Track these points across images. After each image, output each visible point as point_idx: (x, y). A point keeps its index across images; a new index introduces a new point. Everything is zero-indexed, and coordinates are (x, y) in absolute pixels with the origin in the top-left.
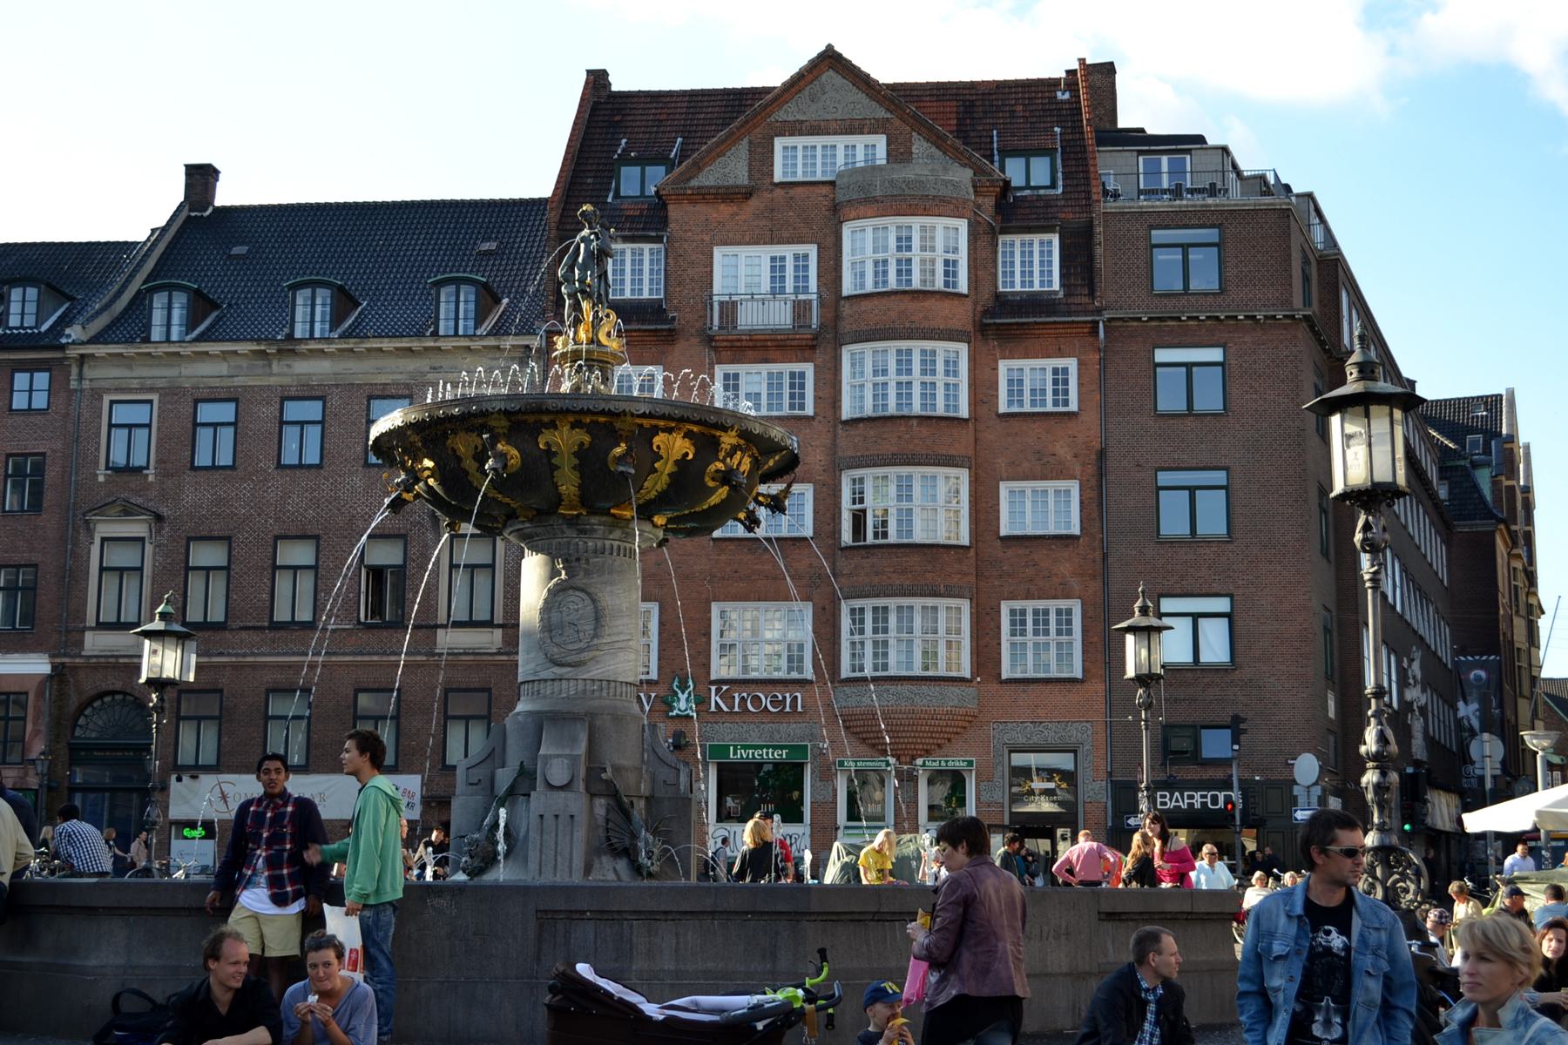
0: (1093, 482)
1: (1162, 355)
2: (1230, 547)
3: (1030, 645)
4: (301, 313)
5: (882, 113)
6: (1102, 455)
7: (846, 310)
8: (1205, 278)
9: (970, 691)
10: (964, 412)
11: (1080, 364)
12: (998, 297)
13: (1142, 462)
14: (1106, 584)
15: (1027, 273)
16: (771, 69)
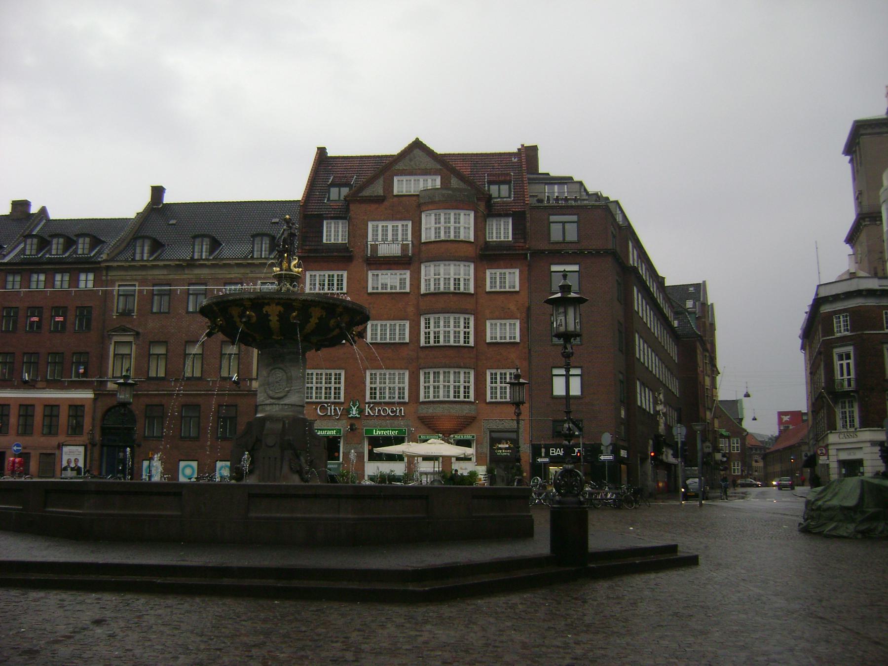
1: (554, 268)
3: (499, 388)
4: (138, 250)
5: (439, 167)
6: (529, 309)
7: (423, 248)
8: (572, 234)
9: (473, 407)
10: (472, 291)
12: (486, 243)
14: (530, 362)
15: (498, 233)
16: (394, 148)
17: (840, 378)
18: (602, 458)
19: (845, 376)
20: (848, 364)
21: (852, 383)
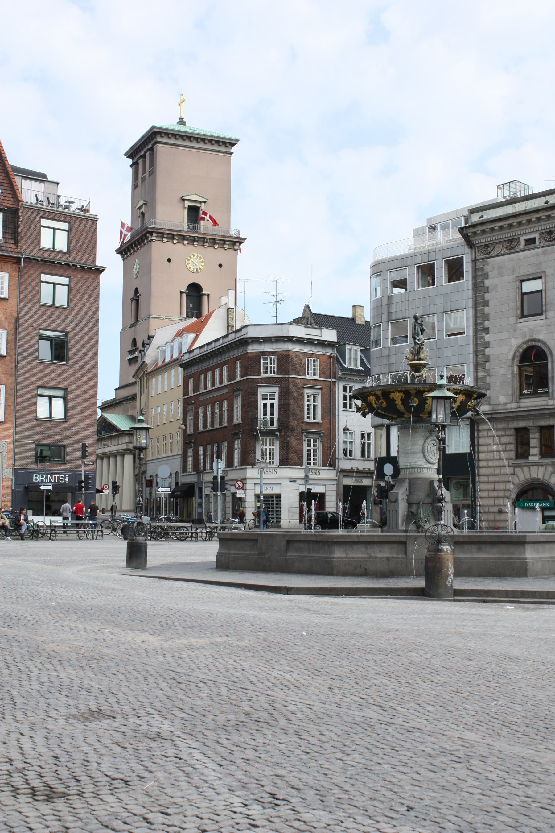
0: (13, 332)
1: (44, 277)
2: (67, 367)
6: (17, 319)
8: (62, 244)
11: (10, 276)
13: (34, 325)
14: (16, 379)
17: (262, 416)
18: (160, 490)
19: (268, 416)
20: (272, 405)
21: (275, 422)
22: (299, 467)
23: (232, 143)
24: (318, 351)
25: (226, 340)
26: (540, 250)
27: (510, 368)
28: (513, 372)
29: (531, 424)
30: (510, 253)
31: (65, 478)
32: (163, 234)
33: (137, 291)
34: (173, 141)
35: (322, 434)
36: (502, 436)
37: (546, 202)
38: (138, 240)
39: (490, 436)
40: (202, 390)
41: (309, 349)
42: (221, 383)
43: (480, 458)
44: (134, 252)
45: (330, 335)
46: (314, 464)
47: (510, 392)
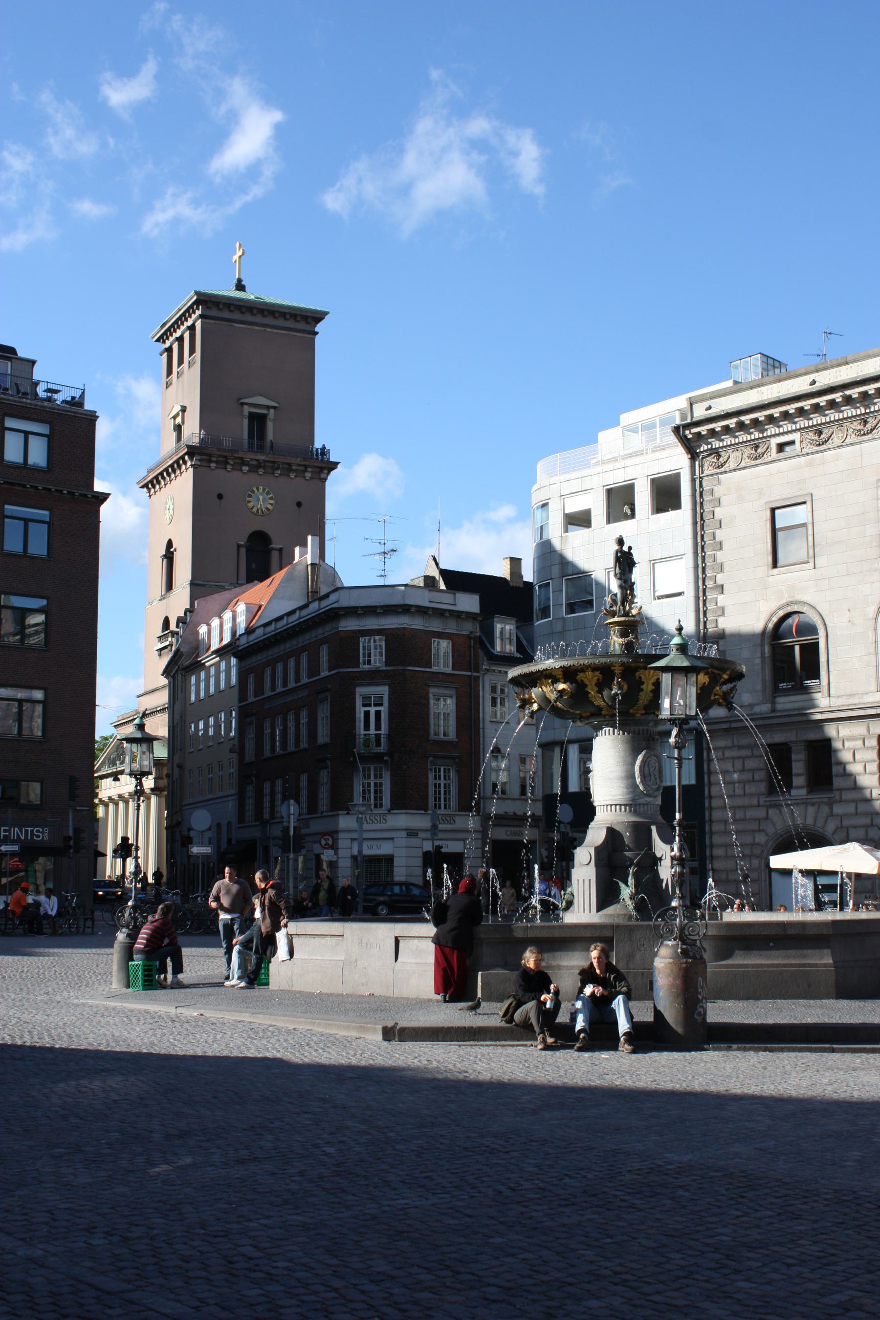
17: (363, 732)
18: (195, 850)
19: (372, 731)
20: (378, 713)
21: (383, 741)
22: (423, 812)
23: (317, 317)
24: (452, 627)
25: (305, 612)
26: (803, 459)
27: (759, 648)
28: (763, 653)
29: (793, 738)
30: (756, 466)
31: (43, 833)
32: (211, 455)
33: (170, 544)
34: (226, 314)
35: (457, 760)
36: (748, 757)
37: (813, 382)
38: (172, 466)
39: (727, 758)
40: (268, 693)
41: (435, 625)
42: (297, 680)
43: (713, 794)
44: (165, 485)
45: (469, 603)
46: (445, 808)
47: (759, 687)
